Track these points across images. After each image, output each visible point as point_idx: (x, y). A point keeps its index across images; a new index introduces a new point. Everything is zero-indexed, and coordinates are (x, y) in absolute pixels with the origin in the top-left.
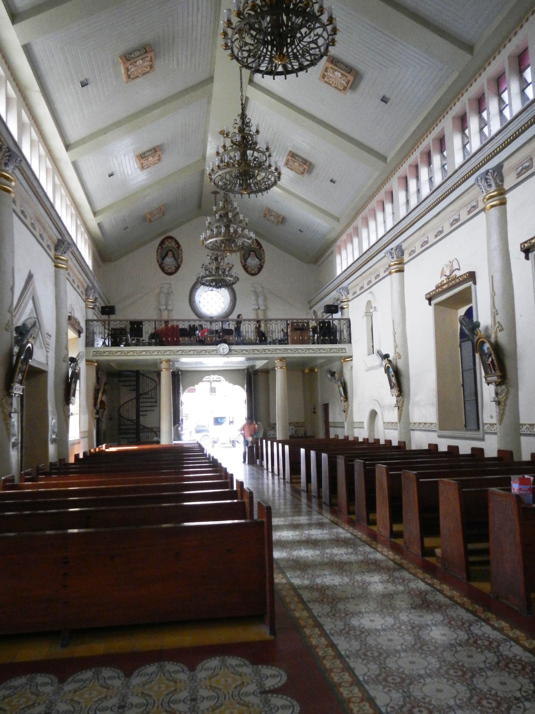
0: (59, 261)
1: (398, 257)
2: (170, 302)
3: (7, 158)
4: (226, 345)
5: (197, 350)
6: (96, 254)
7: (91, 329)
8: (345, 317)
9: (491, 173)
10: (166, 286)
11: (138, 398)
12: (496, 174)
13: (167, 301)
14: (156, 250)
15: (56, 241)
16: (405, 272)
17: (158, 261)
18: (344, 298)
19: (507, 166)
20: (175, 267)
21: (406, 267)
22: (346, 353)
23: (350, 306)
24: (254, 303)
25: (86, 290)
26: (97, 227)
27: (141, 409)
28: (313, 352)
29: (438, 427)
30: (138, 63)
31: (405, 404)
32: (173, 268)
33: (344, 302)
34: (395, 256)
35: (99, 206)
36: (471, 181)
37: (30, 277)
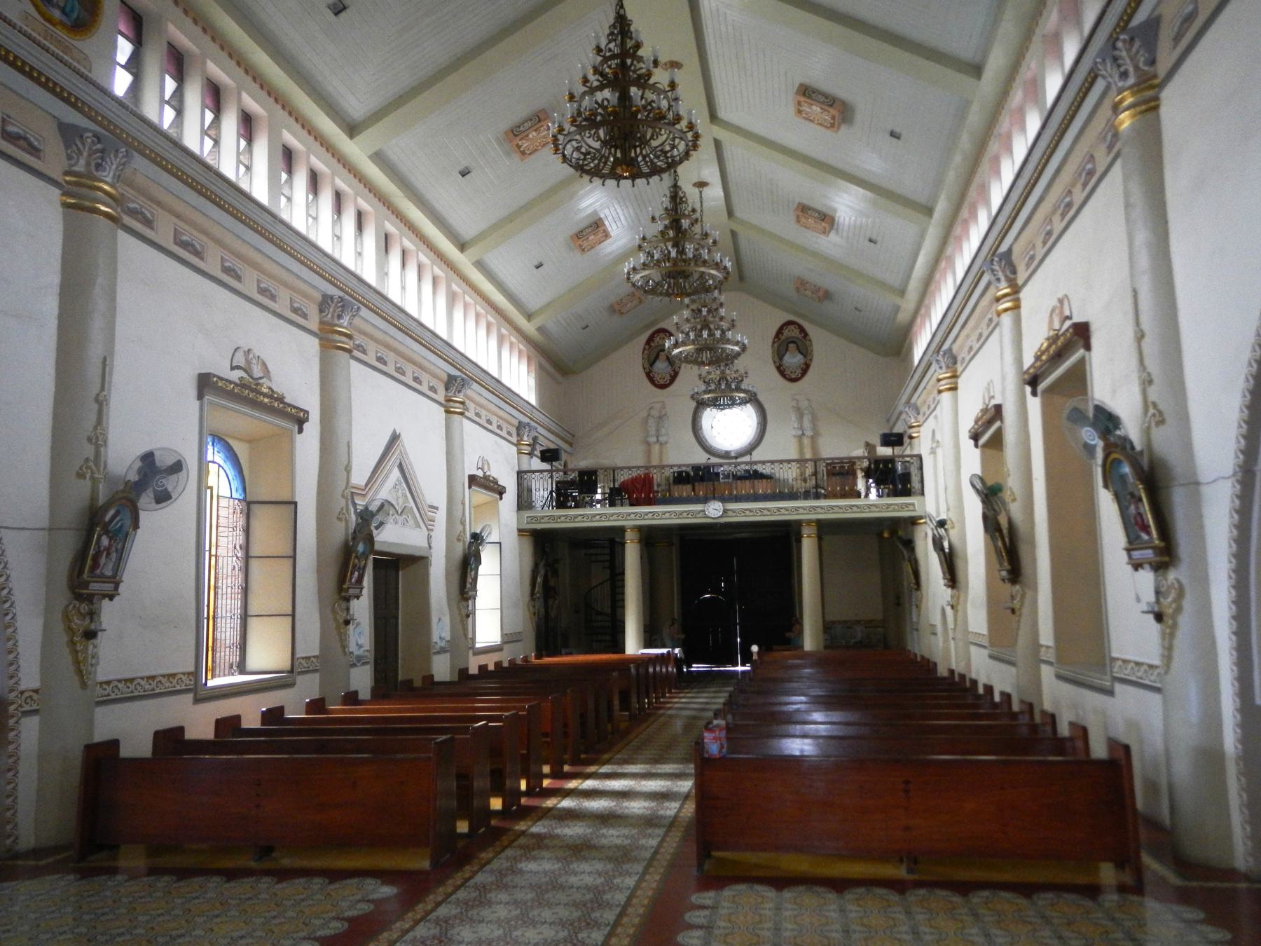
0: (452, 404)
1: (948, 367)
2: (663, 431)
3: (340, 309)
4: (720, 504)
5: (675, 512)
7: (525, 485)
8: (915, 452)
9: (997, 262)
10: (658, 406)
12: (1003, 263)
13: (658, 430)
14: (641, 350)
15: (445, 377)
16: (959, 391)
17: (644, 368)
18: (913, 420)
19: (1016, 250)
20: (671, 376)
21: (960, 381)
22: (915, 510)
23: (921, 434)
25: (518, 429)
26: (536, 332)
28: (858, 510)
29: (990, 642)
30: (531, 136)
31: (961, 599)
32: (668, 378)
33: (914, 427)
34: (943, 365)
35: (534, 303)
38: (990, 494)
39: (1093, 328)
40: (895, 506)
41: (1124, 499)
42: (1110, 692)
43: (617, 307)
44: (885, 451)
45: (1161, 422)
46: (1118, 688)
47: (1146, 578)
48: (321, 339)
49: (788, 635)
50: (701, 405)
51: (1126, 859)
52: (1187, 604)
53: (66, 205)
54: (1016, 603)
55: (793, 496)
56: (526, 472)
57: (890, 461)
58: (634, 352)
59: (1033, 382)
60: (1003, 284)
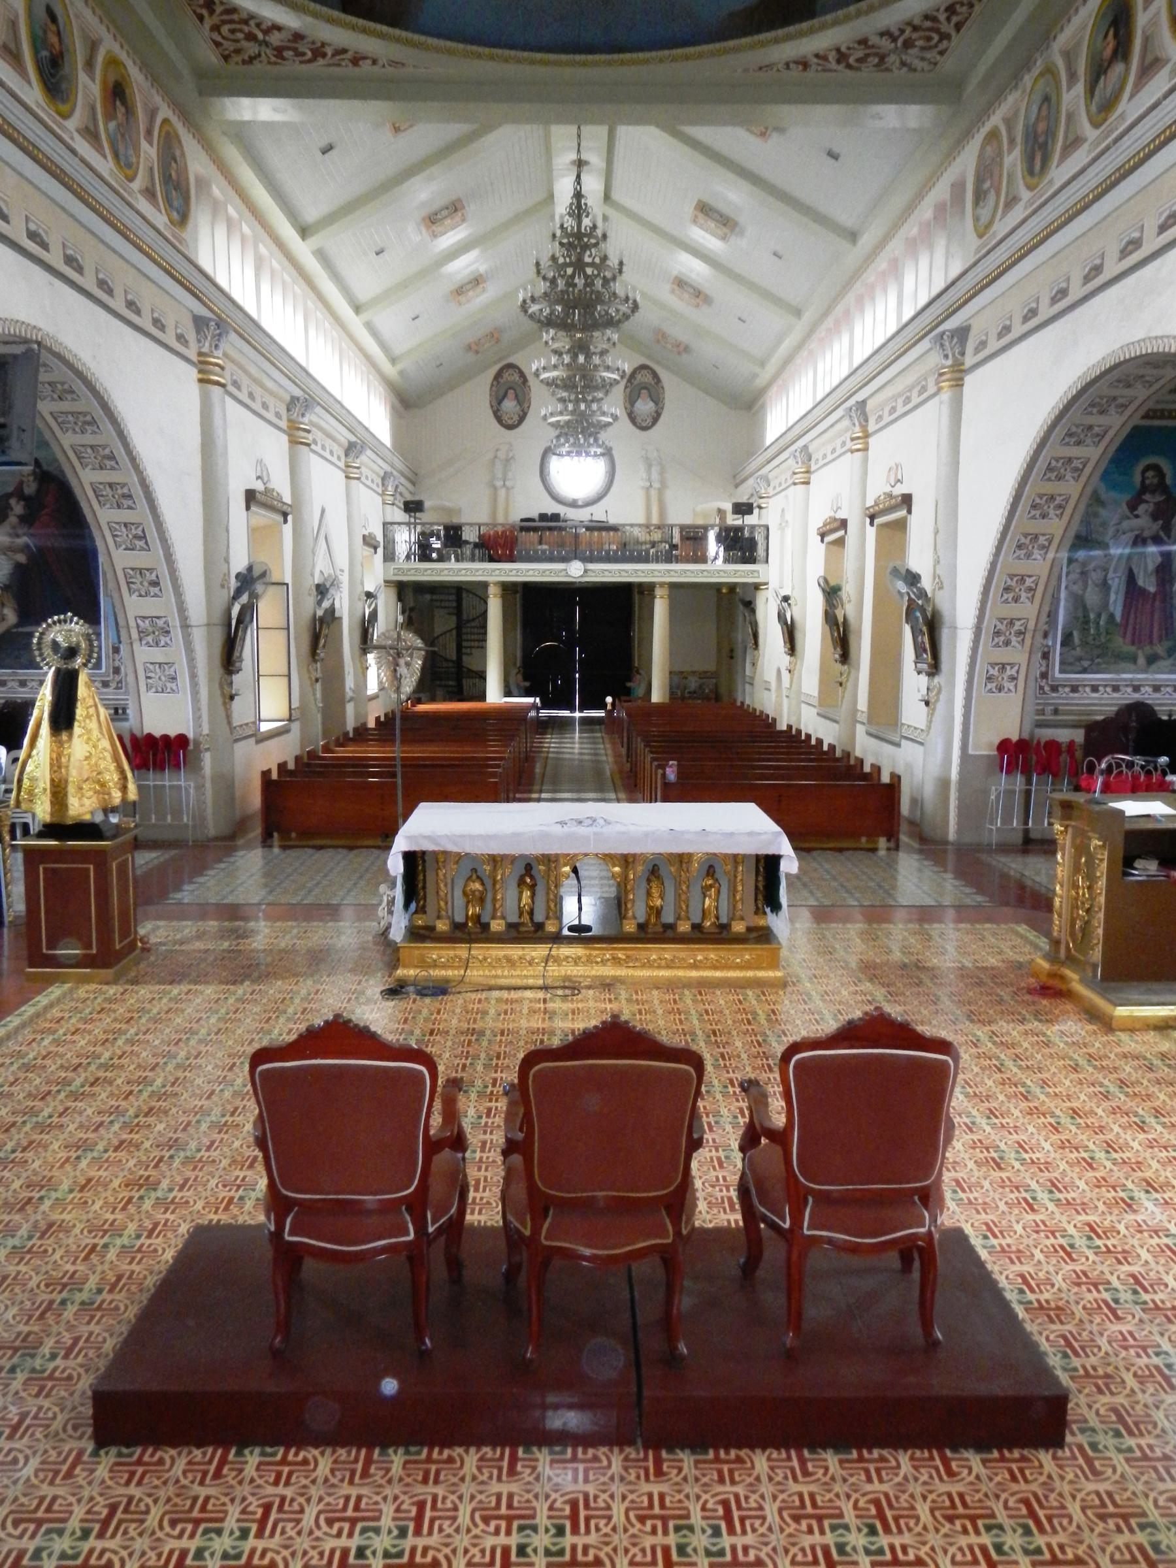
2: (510, 475)
6: (398, 405)
8: (762, 522)
11: (459, 628)
13: (505, 474)
15: (346, 444)
19: (870, 405)
21: (813, 478)
24: (644, 476)
25: (383, 479)
27: (465, 644)
32: (516, 418)
35: (398, 350)
36: (840, 412)
37: (323, 511)
38: (831, 593)
39: (914, 499)
40: (739, 573)
41: (915, 633)
42: (898, 745)
43: (474, 347)
44: (733, 520)
45: (941, 588)
46: (903, 742)
47: (924, 679)
48: (290, 435)
49: (628, 684)
50: (547, 452)
51: (892, 835)
52: (942, 697)
53: (201, 381)
54: (843, 679)
55: (646, 559)
56: (392, 523)
57: (739, 529)
58: (480, 389)
59: (872, 518)
60: (857, 429)
